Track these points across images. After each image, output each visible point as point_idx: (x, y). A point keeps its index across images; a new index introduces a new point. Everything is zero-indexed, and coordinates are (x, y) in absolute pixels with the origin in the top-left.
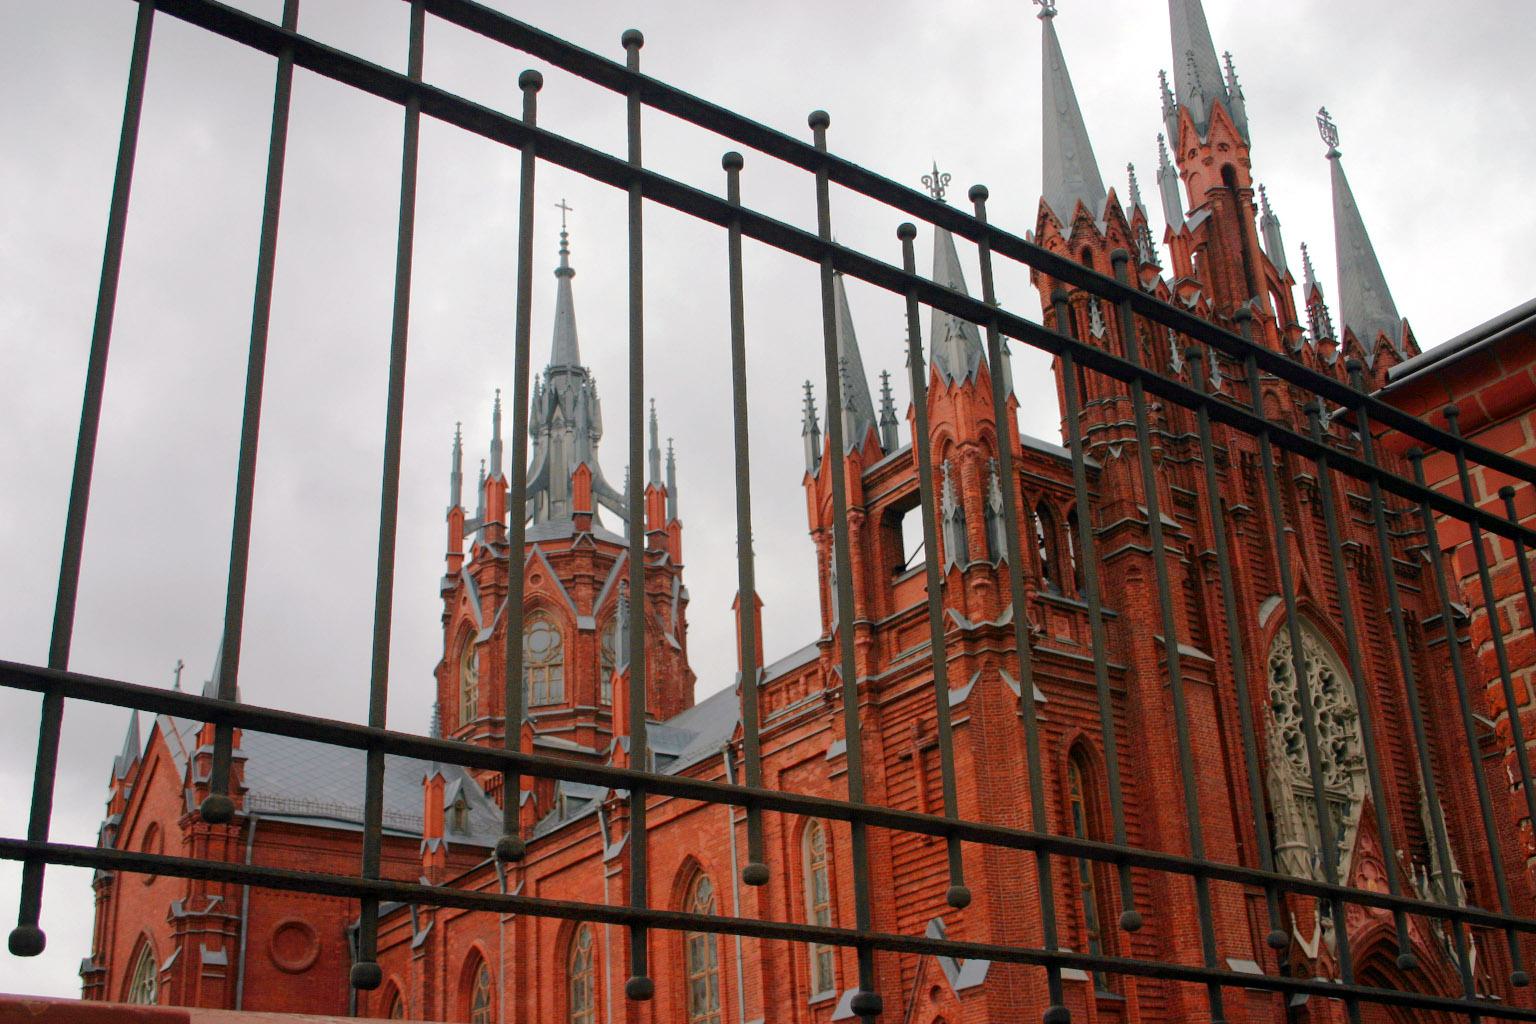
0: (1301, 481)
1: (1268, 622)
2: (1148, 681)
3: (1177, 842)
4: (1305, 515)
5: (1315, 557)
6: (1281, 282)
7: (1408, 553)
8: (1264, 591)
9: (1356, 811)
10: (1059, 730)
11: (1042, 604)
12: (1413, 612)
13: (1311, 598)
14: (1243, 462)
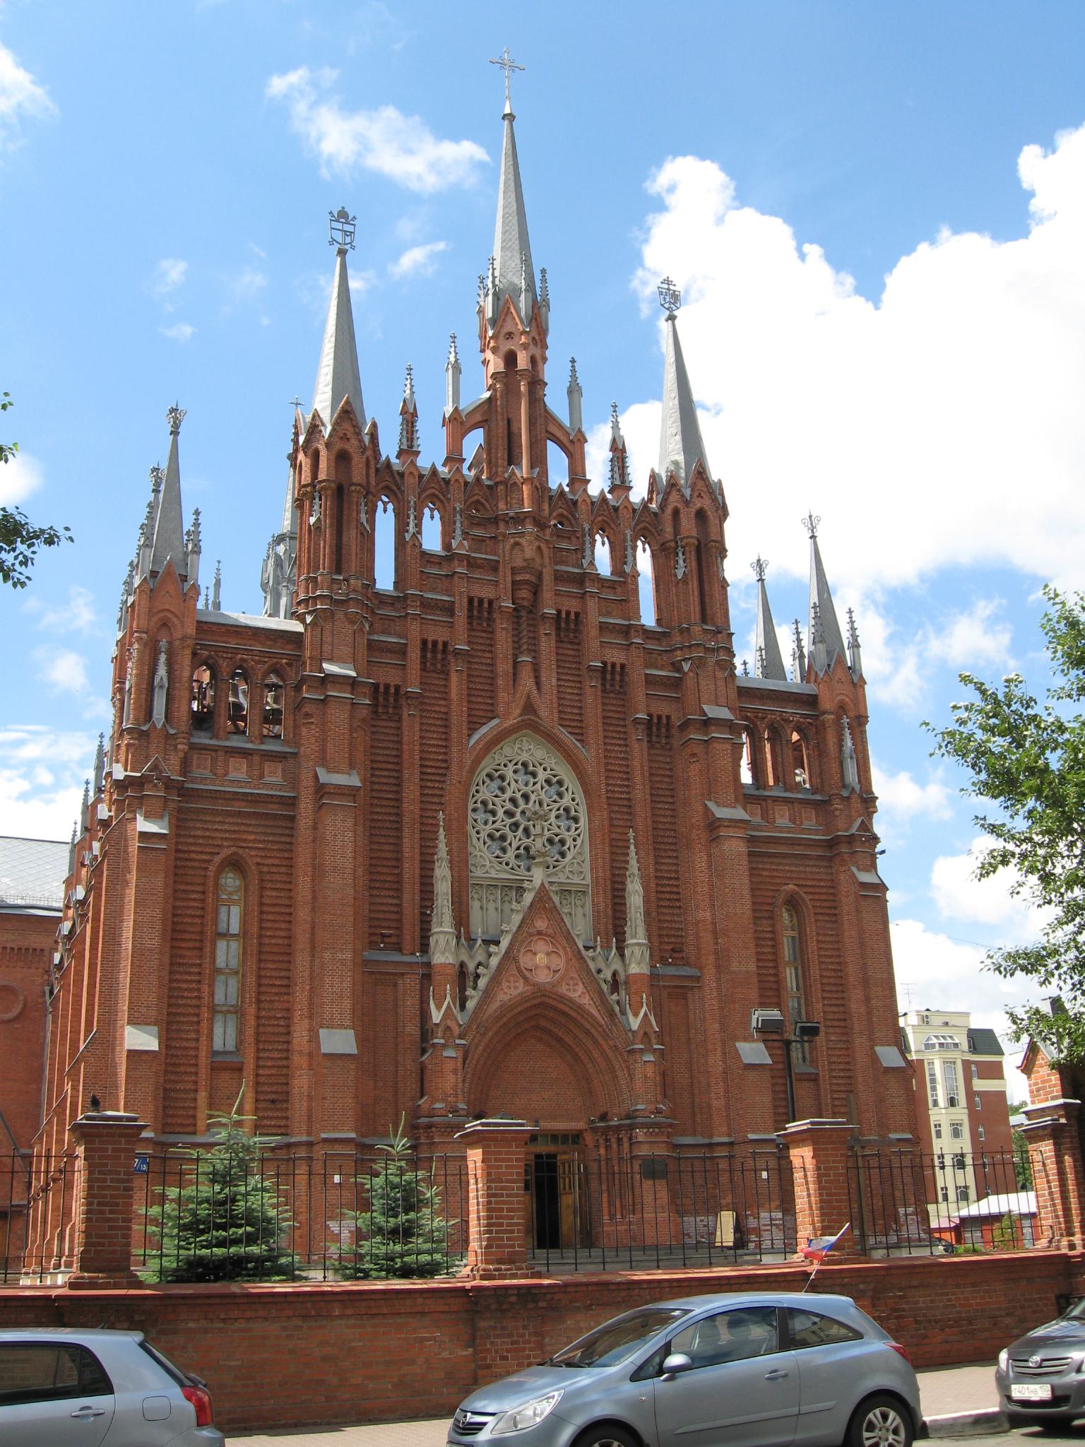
0: (544, 616)
1: (477, 742)
2: (306, 806)
3: (308, 935)
4: (547, 645)
5: (550, 679)
6: (572, 442)
7: (673, 664)
8: (489, 715)
9: (528, 898)
10: (217, 850)
11: (216, 751)
12: (668, 717)
13: (538, 716)
14: (470, 609)
